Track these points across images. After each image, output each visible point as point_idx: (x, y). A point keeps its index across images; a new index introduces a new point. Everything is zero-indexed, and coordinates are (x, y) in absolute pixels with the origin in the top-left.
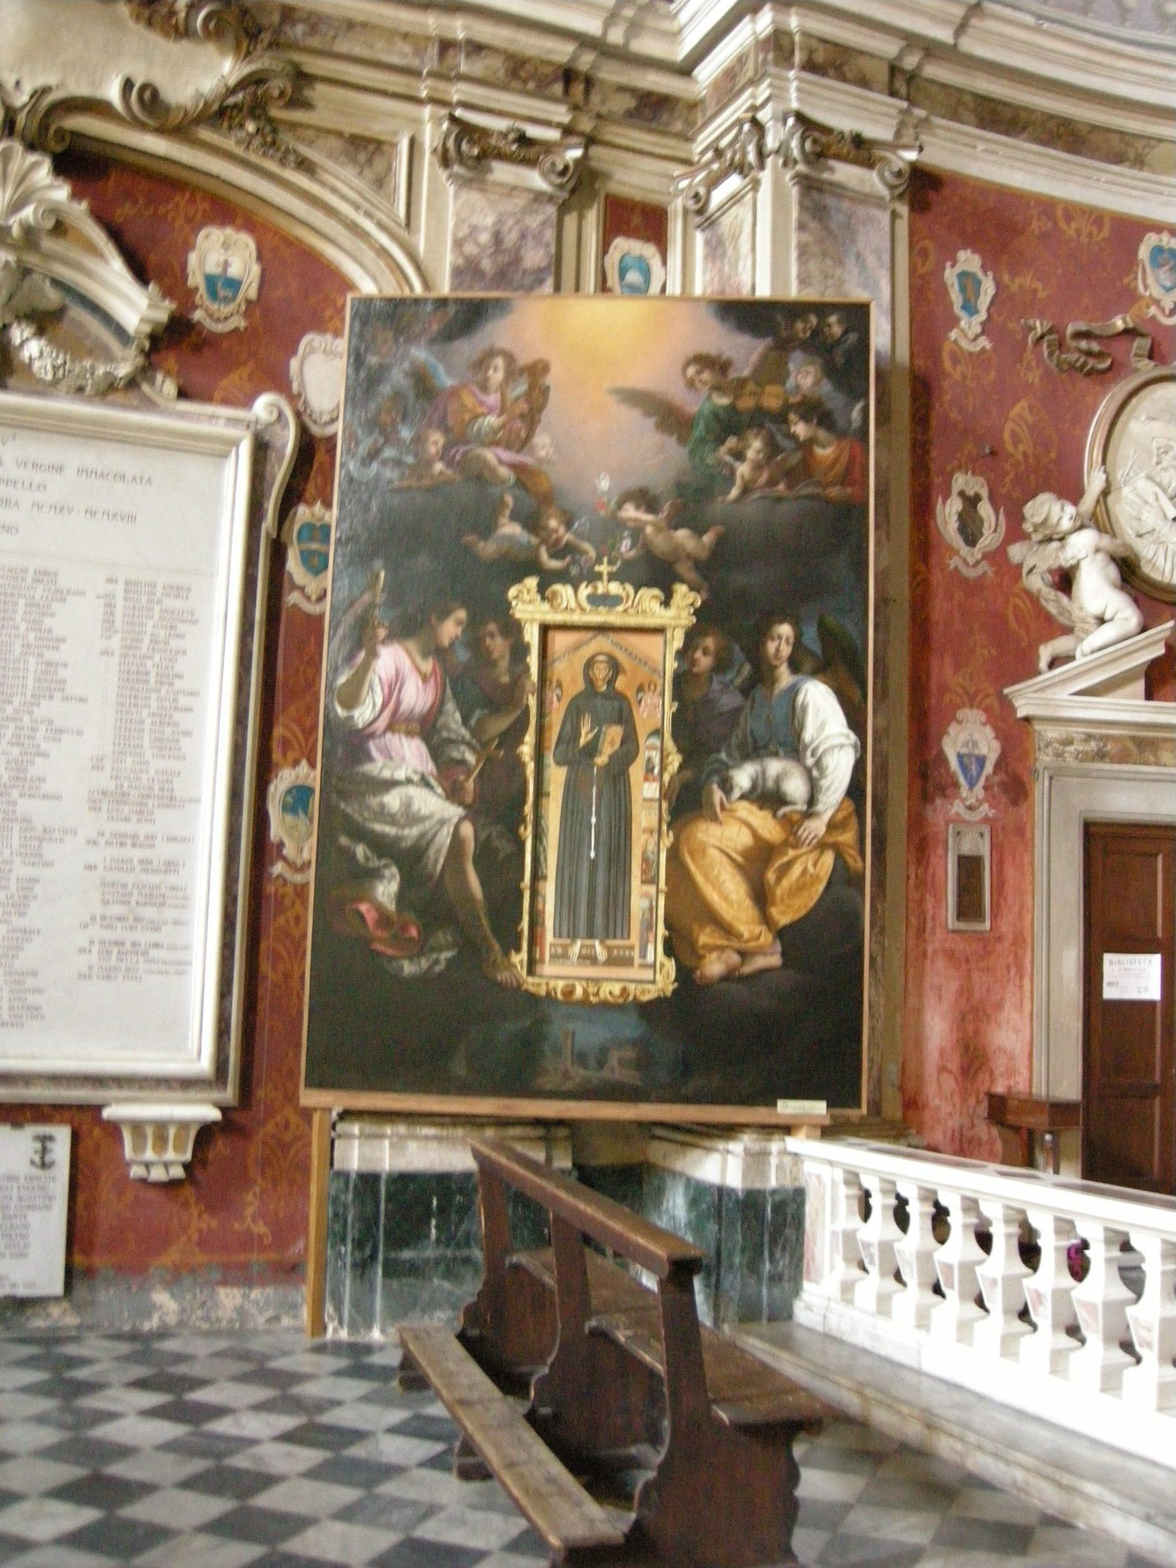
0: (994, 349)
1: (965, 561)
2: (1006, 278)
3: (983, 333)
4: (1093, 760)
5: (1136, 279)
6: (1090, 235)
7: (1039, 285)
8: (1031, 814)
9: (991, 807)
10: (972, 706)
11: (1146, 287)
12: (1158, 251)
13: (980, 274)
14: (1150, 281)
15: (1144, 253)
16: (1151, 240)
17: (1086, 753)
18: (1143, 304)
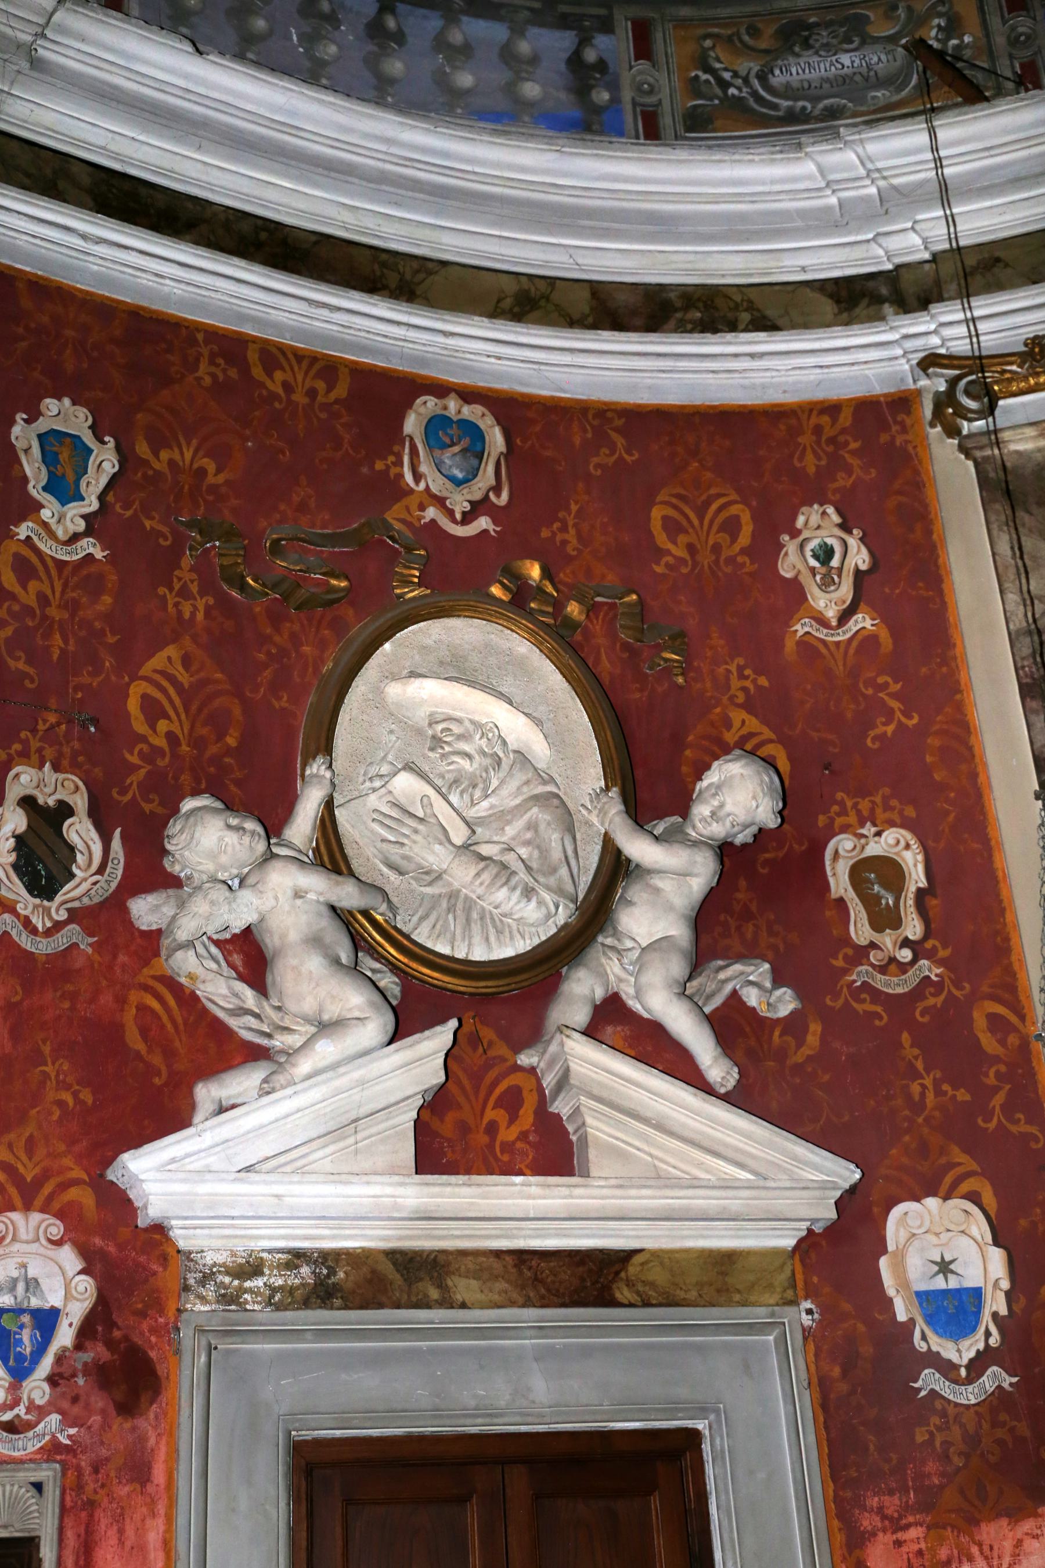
0: (111, 559)
1: (27, 923)
2: (143, 449)
3: (88, 532)
4: (306, 1304)
5: (401, 464)
6: (312, 393)
7: (211, 467)
8: (171, 1434)
9: (68, 1421)
10: (27, 1207)
11: (417, 477)
12: (436, 425)
13: (88, 439)
14: (423, 468)
15: (412, 424)
16: (427, 405)
17: (291, 1290)
18: (413, 501)
